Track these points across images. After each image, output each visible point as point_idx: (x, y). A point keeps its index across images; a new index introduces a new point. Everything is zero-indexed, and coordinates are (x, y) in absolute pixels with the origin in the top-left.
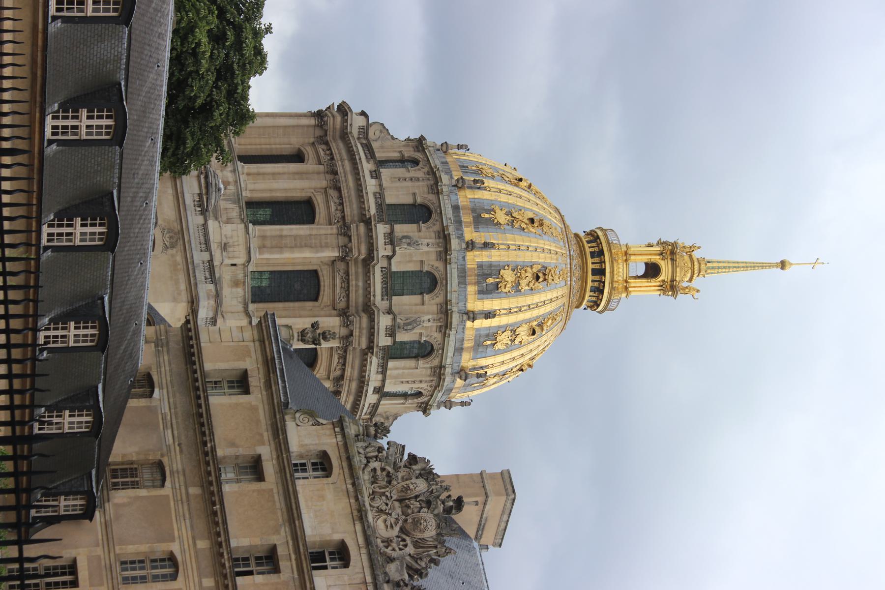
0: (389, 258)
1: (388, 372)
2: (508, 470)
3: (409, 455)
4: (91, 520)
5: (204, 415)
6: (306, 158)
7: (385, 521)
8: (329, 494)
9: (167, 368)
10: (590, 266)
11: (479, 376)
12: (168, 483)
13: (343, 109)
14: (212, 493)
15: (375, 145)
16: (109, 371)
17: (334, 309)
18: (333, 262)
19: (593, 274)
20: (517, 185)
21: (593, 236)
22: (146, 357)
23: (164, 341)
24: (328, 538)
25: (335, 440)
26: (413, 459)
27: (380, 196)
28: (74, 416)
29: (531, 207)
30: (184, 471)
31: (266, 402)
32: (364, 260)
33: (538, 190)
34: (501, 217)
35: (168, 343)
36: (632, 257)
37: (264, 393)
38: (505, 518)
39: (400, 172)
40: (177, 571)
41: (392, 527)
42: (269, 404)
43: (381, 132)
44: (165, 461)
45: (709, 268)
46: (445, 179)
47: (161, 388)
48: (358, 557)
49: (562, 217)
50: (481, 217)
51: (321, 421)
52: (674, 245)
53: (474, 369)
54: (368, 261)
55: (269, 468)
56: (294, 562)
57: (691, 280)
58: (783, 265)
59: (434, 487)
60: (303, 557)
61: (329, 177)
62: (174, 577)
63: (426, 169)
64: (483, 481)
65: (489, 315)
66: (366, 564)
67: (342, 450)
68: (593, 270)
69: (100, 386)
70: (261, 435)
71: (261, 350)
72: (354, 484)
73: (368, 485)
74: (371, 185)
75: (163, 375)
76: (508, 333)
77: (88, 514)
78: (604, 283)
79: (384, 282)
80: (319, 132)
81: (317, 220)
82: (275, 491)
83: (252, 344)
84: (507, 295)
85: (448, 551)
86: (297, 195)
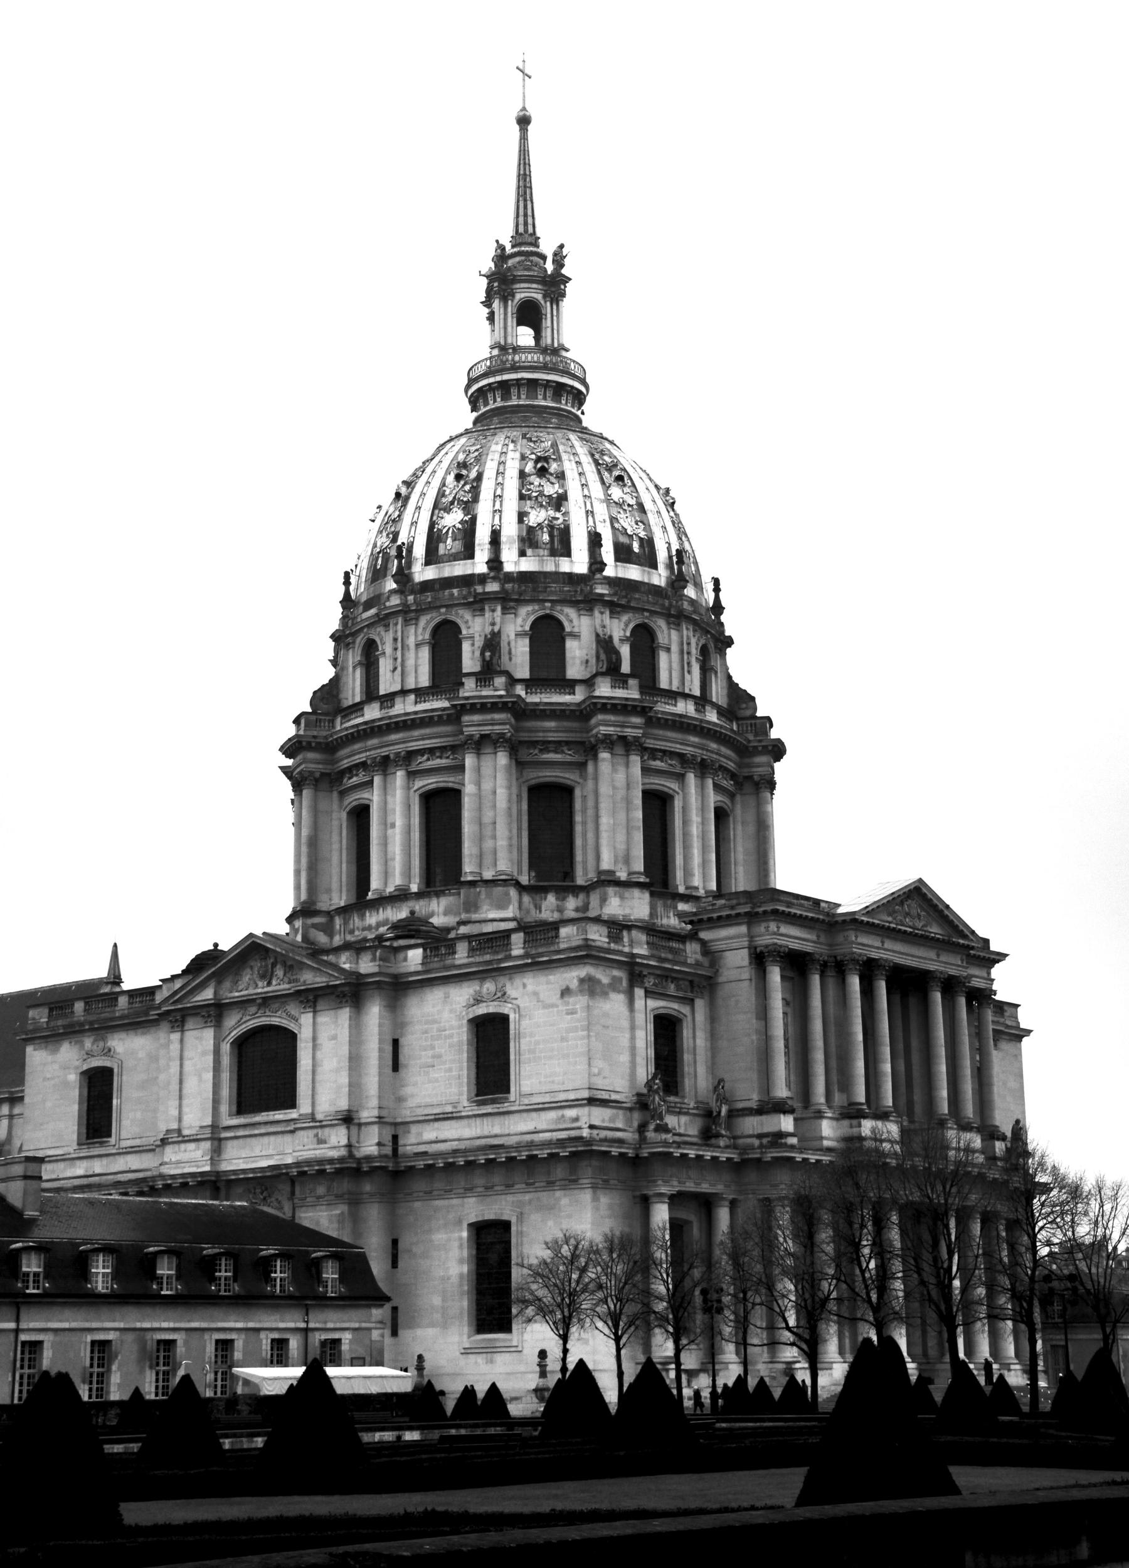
0: (512, 681)
1: (674, 688)
11: (680, 562)
18: (519, 765)
29: (441, 473)
34: (453, 519)
36: (509, 341)
39: (385, 666)
49: (451, 439)
53: (670, 566)
54: (520, 711)
57: (544, 258)
63: (380, 629)
65: (595, 540)
74: (406, 707)
78: (548, 381)
81: (456, 786)
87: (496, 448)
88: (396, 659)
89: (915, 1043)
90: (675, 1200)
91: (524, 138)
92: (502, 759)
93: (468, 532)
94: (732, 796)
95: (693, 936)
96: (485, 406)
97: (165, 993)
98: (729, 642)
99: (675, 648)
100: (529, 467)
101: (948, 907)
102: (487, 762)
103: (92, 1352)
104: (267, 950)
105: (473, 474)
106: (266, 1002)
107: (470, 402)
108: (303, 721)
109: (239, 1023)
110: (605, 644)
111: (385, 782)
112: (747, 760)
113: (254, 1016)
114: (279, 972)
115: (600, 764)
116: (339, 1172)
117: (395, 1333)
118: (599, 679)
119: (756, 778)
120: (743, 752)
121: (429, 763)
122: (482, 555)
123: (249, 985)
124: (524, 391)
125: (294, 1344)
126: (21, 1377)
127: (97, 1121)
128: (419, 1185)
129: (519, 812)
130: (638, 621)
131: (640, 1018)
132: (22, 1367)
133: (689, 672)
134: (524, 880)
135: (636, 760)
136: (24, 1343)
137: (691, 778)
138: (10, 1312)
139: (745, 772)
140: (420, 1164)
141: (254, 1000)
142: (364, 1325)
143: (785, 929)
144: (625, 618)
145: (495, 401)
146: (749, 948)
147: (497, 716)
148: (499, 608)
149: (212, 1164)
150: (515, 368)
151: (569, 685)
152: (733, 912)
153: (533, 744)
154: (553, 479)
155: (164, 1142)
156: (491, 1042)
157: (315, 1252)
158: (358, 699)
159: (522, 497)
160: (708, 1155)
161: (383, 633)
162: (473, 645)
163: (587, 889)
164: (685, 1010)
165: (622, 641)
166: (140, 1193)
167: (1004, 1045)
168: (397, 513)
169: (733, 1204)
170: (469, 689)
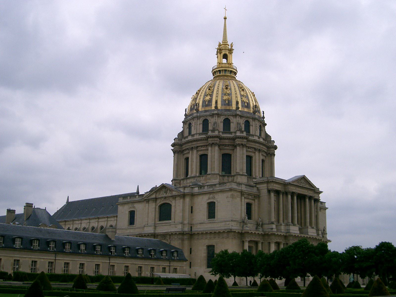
1: (254, 134)
11: (255, 107)
17: (234, 149)
18: (220, 149)
21: (214, 74)
27: (200, 134)
32: (220, 140)
36: (221, 62)
39: (193, 128)
46: (195, 115)
49: (208, 82)
53: (254, 109)
57: (229, 45)
58: (225, 18)
61: (193, 150)
65: (237, 103)
78: (229, 70)
81: (207, 154)
88: (195, 127)
89: (303, 210)
90: (250, 242)
91: (225, 22)
92: (217, 148)
93: (210, 101)
94: (266, 157)
95: (256, 186)
96: (216, 75)
97: (146, 195)
98: (266, 125)
99: (254, 125)
100: (224, 87)
101: (310, 181)
103: (125, 268)
104: (166, 187)
105: (212, 89)
106: (165, 198)
107: (213, 74)
108: (176, 139)
109: (160, 202)
110: (238, 124)
111: (192, 153)
112: (269, 150)
113: (163, 201)
114: (168, 191)
115: (237, 149)
116: (180, 234)
117: (190, 267)
118: (238, 132)
119: (271, 153)
120: (269, 148)
121: (201, 149)
123: (162, 194)
124: (224, 72)
125: (167, 269)
126: (110, 272)
127: (132, 221)
128: (196, 237)
129: (220, 160)
130: (246, 120)
131: (243, 203)
132: (111, 270)
133: (257, 130)
134: (221, 174)
135: (245, 149)
136: (111, 265)
137: (257, 153)
138: (108, 259)
139: (269, 152)
140: (196, 233)
141: (163, 197)
142: (182, 265)
143: (275, 185)
144: (243, 119)
146: (267, 189)
147: (216, 139)
148: (217, 116)
149: (154, 231)
150: (222, 67)
151: (231, 133)
152: (264, 181)
153: (223, 145)
154: (229, 90)
155: (144, 226)
156: (211, 207)
157: (172, 250)
158: (187, 135)
159: (222, 94)
160: (257, 233)
161: (193, 121)
162: (211, 124)
163: (234, 176)
164: (253, 202)
165: (243, 124)
166: (140, 237)
167: (322, 211)
168: (196, 97)
169: (262, 243)
170: (210, 133)
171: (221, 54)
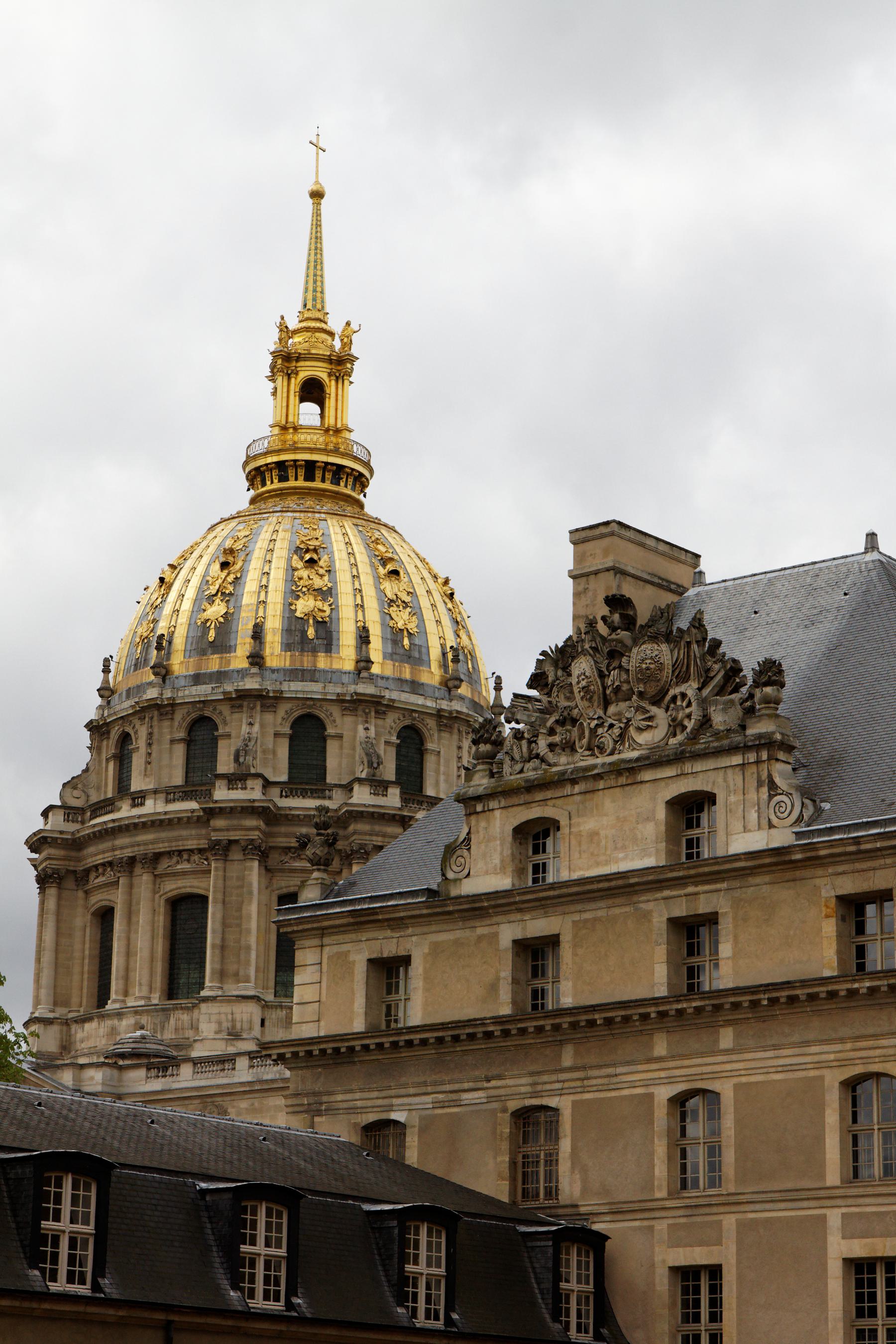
0: (267, 784)
2: (571, 532)
3: (530, 686)
4: (605, 1238)
5: (440, 1034)
6: (104, 903)
7: (640, 730)
8: (588, 824)
9: (358, 1095)
10: (301, 483)
12: (553, 1102)
13: (36, 843)
14: (574, 1025)
15: (94, 798)
16: (342, 1190)
18: (268, 870)
19: (313, 480)
20: (170, 586)
21: (254, 477)
22: (338, 1130)
23: (312, 1100)
24: (663, 828)
25: (497, 813)
26: (536, 681)
28: (416, 1257)
30: (532, 1074)
31: (425, 929)
32: (267, 824)
33: (179, 555)
34: (217, 610)
35: (315, 1094)
36: (291, 419)
37: (410, 931)
38: (651, 543)
39: (137, 761)
40: (704, 1092)
41: (650, 718)
42: (429, 924)
43: (75, 788)
44: (514, 1105)
45: (314, 306)
46: (152, 693)
47: (390, 1108)
48: (698, 777)
49: (223, 520)
50: (214, 640)
51: (463, 836)
52: (275, 354)
53: (444, 665)
54: (271, 816)
55: (538, 926)
56: (700, 888)
57: (331, 334)
58: (317, 195)
59: (587, 646)
60: (692, 872)
61: (138, 870)
62: (711, 1097)
63: (137, 722)
64: (586, 575)
65: (363, 638)
66: (710, 764)
67: (515, 800)
68: (306, 479)
69: (367, 1207)
70: (480, 938)
71: (336, 933)
72: (574, 782)
73: (577, 757)
75: (369, 1103)
76: (393, 610)
77: (596, 1243)
78: (327, 464)
79: (304, 794)
80: (70, 883)
82: (576, 917)
83: (326, 950)
84: (334, 608)
85: (698, 623)
86: (161, 920)
87: (265, 535)
102: (234, 869)
107: (247, 479)
122: (243, 647)
145: (272, 482)
168: (160, 600)
171: (293, 380)
